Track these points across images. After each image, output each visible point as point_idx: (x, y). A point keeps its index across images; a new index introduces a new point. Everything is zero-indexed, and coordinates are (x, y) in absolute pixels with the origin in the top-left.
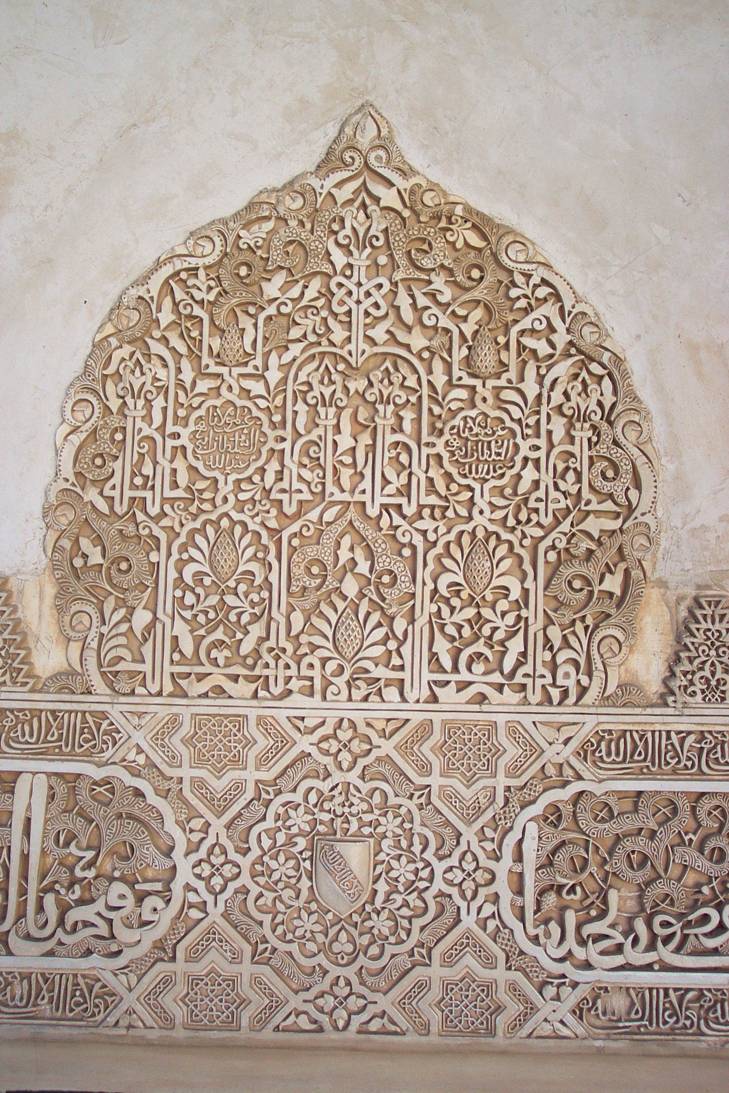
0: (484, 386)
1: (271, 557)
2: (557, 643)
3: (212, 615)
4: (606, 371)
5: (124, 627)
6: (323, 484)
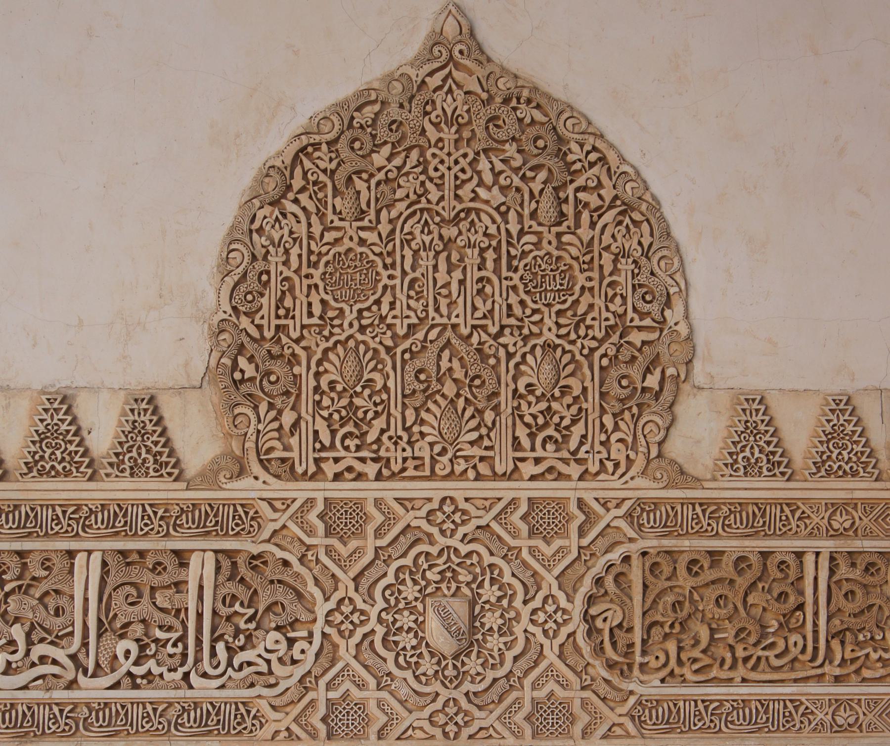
0: (550, 232)
1: (389, 369)
2: (610, 429)
3: (344, 413)
4: (644, 218)
5: (275, 425)
6: (427, 312)
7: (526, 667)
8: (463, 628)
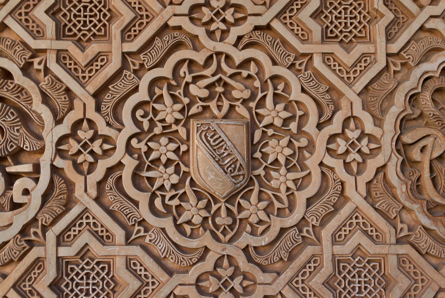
7: (324, 213)
8: (240, 161)
